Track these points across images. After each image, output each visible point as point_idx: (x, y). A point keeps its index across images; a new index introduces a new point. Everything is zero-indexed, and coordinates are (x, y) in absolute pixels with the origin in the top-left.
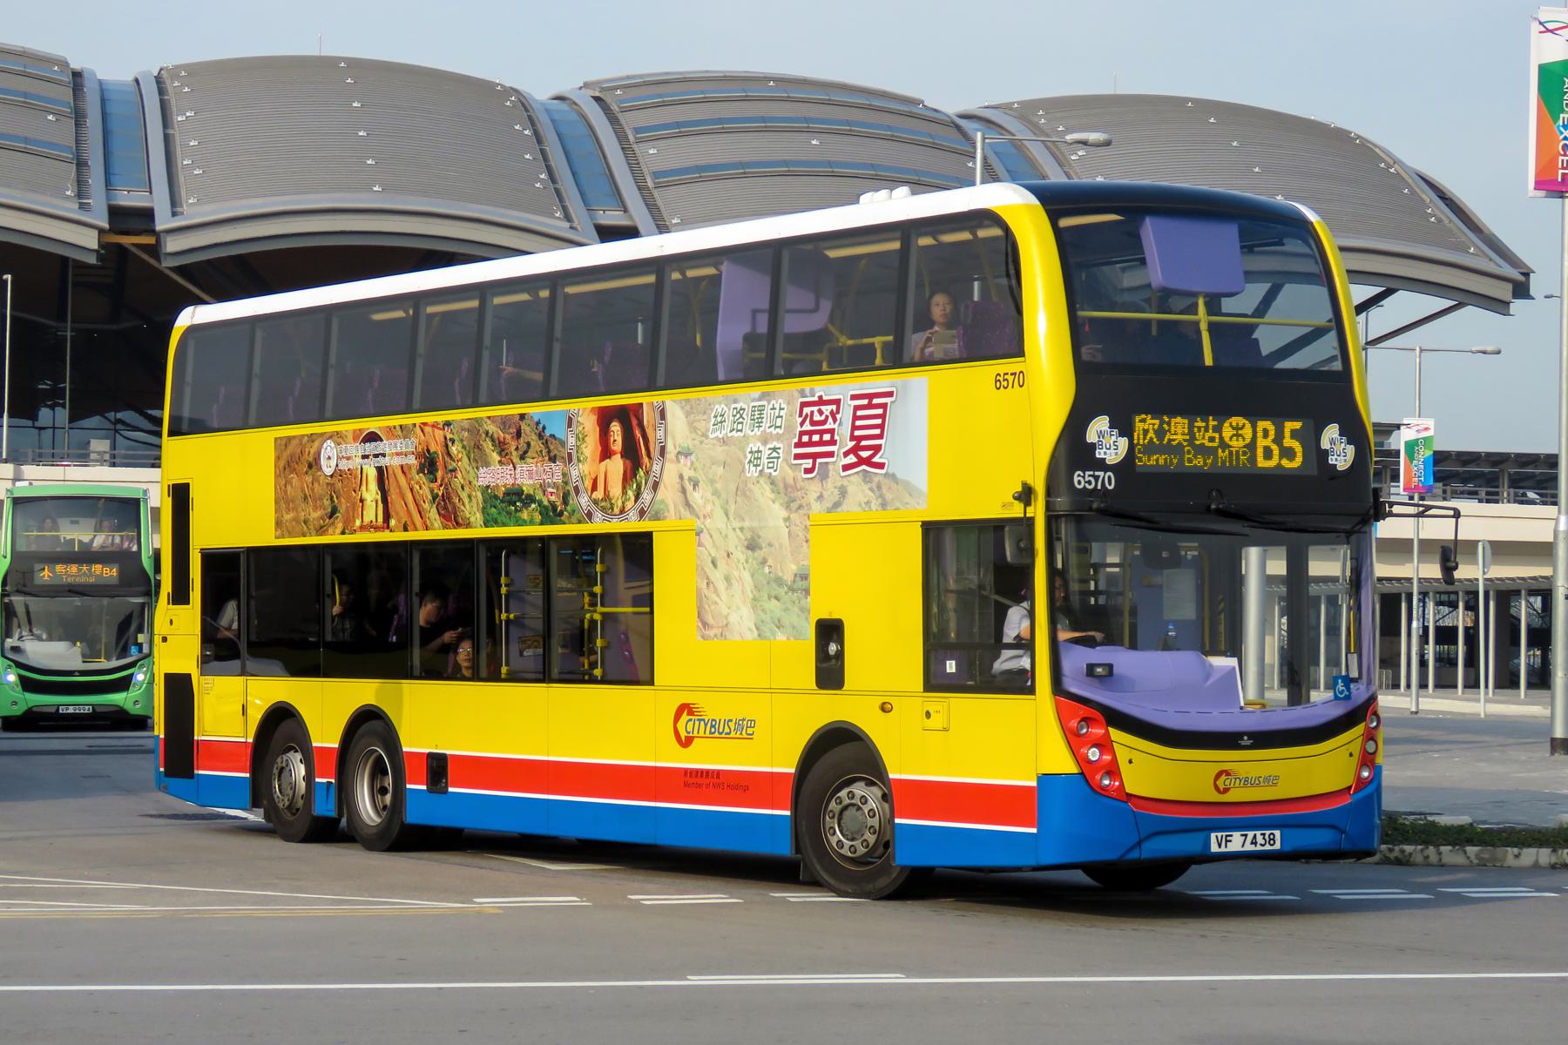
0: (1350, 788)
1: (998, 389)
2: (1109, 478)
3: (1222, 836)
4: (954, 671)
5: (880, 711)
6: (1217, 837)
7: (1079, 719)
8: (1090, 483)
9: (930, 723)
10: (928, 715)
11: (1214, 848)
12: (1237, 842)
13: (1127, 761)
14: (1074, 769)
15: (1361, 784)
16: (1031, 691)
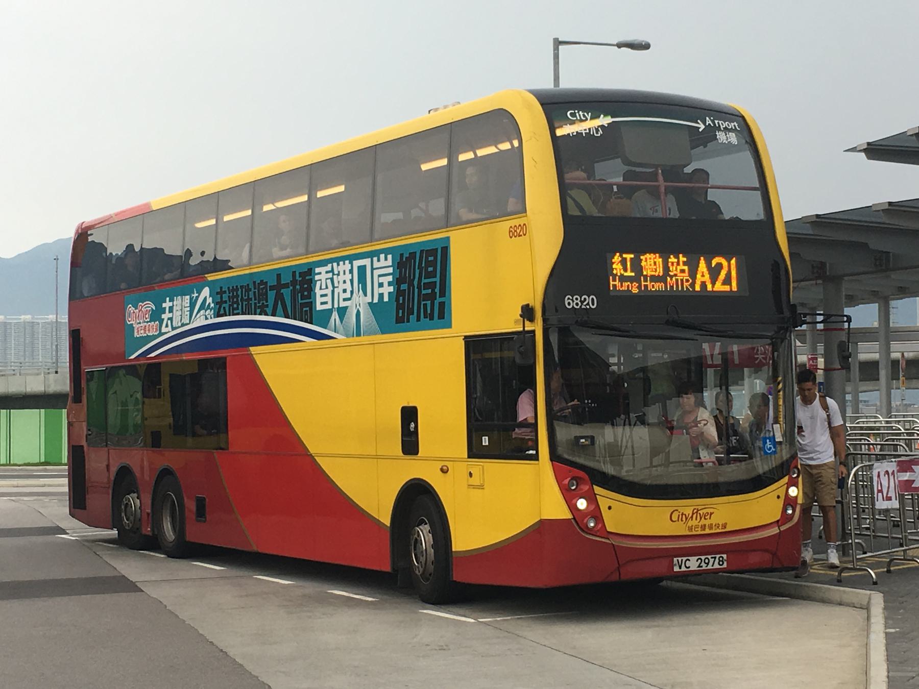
0: (778, 521)
1: (511, 237)
2: (593, 299)
3: (682, 560)
4: (487, 444)
5: (441, 472)
6: (678, 560)
7: (569, 479)
8: (577, 304)
9: (472, 481)
10: (471, 475)
11: (676, 569)
12: (693, 564)
13: (607, 507)
14: (570, 518)
15: (785, 518)
16: (535, 458)
